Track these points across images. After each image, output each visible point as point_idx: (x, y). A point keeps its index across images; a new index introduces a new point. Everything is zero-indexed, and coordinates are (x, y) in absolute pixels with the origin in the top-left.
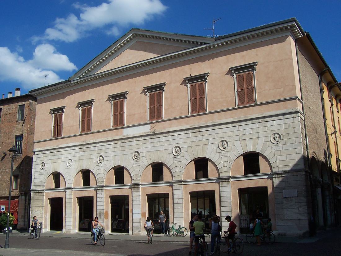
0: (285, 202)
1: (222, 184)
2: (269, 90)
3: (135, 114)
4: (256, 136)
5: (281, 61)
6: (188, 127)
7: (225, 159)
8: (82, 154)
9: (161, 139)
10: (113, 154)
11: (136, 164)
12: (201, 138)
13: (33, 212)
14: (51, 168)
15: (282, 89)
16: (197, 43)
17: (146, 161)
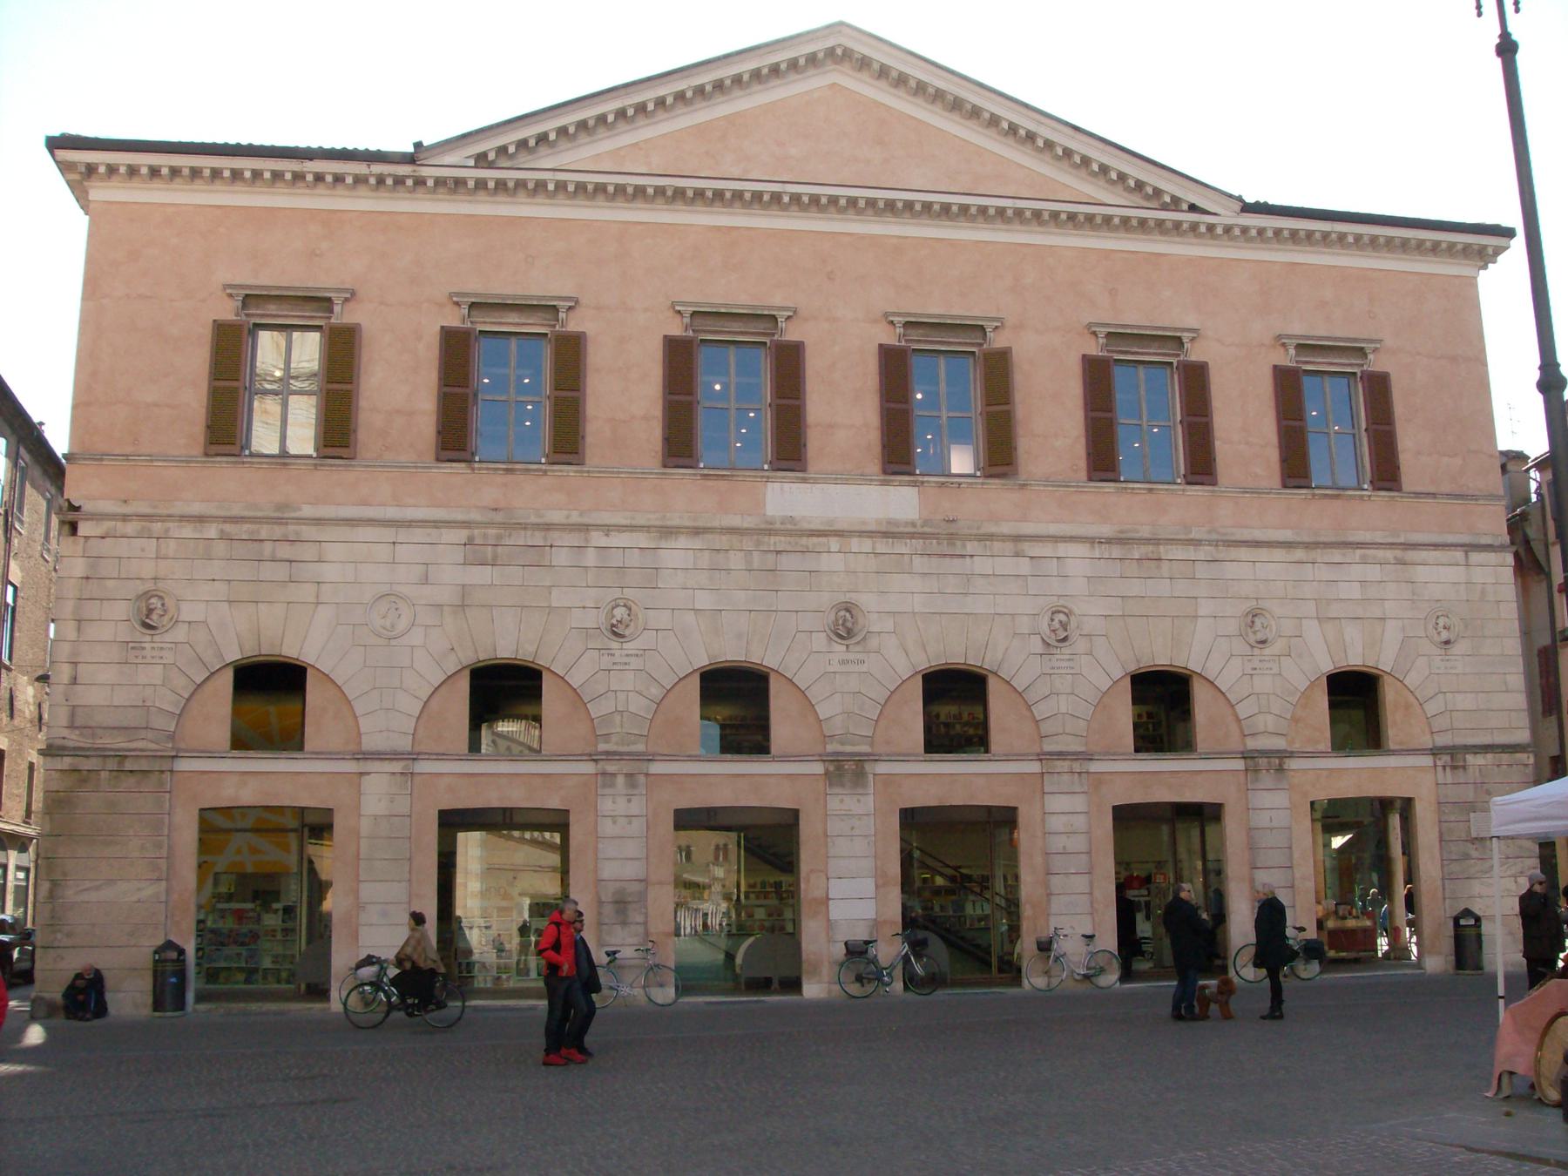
0: (1475, 854)
1: (1257, 780)
3: (831, 426)
4: (1376, 611)
6: (1106, 530)
7: (1263, 684)
8: (480, 575)
9: (981, 565)
10: (704, 600)
11: (844, 662)
12: (1163, 588)
13: (70, 893)
16: (1158, 192)
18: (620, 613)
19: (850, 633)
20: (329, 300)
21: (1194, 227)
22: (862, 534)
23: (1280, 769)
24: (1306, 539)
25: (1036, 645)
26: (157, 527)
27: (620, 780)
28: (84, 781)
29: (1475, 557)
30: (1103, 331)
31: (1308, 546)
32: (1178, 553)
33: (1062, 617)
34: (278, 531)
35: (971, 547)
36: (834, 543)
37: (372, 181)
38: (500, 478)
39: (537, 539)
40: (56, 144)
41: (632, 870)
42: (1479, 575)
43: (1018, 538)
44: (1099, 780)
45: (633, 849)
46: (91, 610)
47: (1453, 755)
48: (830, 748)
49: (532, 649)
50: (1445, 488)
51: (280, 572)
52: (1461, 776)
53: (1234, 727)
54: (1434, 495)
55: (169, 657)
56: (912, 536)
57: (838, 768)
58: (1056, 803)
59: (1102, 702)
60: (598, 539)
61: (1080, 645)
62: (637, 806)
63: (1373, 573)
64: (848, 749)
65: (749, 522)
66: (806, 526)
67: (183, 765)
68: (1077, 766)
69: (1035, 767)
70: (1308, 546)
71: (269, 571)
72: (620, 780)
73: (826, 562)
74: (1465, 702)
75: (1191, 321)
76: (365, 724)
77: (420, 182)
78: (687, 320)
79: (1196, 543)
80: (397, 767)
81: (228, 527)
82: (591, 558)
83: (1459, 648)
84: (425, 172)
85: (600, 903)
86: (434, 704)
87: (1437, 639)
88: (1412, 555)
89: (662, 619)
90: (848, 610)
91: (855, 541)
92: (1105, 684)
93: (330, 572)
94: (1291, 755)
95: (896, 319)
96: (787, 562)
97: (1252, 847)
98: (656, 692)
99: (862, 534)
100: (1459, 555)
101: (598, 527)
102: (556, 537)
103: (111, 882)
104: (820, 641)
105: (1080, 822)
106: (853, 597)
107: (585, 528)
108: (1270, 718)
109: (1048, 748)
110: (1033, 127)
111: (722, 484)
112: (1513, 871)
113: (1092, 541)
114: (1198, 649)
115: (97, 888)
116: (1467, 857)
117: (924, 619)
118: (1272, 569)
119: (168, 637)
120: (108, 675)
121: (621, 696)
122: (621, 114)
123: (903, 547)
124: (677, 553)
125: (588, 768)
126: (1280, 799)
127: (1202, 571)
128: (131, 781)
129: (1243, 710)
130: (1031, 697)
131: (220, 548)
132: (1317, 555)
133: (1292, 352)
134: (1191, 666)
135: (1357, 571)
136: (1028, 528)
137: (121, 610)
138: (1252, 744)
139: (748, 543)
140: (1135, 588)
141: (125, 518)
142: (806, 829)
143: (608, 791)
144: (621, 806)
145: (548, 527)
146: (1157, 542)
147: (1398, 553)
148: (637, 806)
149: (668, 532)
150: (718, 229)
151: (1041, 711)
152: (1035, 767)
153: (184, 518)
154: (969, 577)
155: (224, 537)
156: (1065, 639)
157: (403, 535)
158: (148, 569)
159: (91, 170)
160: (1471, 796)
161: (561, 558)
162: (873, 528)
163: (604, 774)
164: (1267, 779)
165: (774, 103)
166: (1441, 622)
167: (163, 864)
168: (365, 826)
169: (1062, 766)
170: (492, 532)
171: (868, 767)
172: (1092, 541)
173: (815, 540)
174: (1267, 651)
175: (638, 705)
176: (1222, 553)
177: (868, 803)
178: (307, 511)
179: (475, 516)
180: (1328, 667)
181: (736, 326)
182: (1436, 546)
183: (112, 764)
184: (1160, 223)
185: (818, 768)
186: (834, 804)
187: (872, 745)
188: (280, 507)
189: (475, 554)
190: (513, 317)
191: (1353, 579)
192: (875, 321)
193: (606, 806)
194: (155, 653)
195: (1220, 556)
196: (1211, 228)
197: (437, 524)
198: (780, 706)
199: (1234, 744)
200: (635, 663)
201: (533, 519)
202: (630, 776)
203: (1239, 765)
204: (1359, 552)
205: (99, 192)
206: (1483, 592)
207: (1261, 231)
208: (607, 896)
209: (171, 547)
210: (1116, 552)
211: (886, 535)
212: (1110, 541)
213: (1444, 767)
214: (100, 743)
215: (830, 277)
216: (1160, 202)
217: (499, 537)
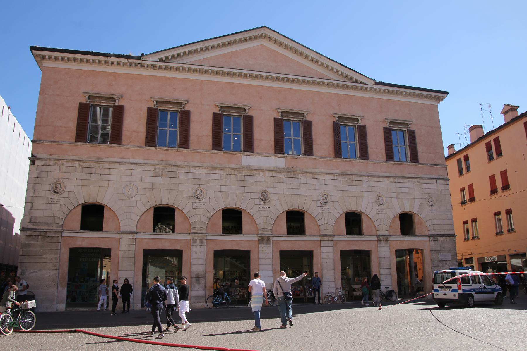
0: (441, 265)
1: (380, 243)
5: (432, 127)
6: (338, 172)
9: (303, 181)
10: (224, 189)
11: (263, 208)
15: (434, 155)
16: (352, 78)
17: (280, 207)
18: (199, 192)
20: (115, 98)
21: (362, 88)
23: (387, 241)
25: (319, 204)
26: (60, 163)
27: (198, 241)
29: (439, 182)
30: (337, 116)
32: (357, 178)
34: (97, 165)
36: (261, 173)
37: (129, 64)
38: (164, 152)
40: (33, 49)
41: (201, 268)
43: (313, 173)
44: (336, 243)
45: (202, 261)
47: (435, 237)
48: (260, 232)
49: (172, 202)
50: (430, 163)
51: (97, 177)
52: (436, 243)
53: (374, 228)
54: (427, 164)
56: (283, 172)
57: (262, 238)
58: (324, 249)
60: (193, 170)
61: (331, 204)
63: (411, 185)
64: (265, 233)
67: (64, 235)
69: (318, 239)
70: (394, 177)
71: (93, 177)
72: (198, 241)
73: (259, 179)
74: (436, 222)
76: (121, 223)
77: (142, 66)
78: (220, 108)
79: (363, 175)
80: (131, 236)
82: (190, 176)
83: (435, 207)
84: (144, 62)
85: (192, 278)
86: (143, 218)
88: (421, 181)
89: (210, 194)
90: (265, 193)
92: (338, 215)
93: (113, 178)
95: (279, 110)
96: (248, 178)
97: (380, 263)
98: (209, 215)
104: (257, 201)
105: (331, 255)
107: (189, 167)
109: (322, 233)
110: (318, 58)
114: (364, 205)
115: (36, 272)
116: (439, 266)
117: (288, 195)
118: (383, 184)
119: (62, 196)
121: (199, 216)
122: (201, 50)
123: (281, 175)
124: (216, 175)
125: (189, 237)
126: (387, 249)
127: (365, 184)
128: (49, 239)
129: (376, 224)
130: (317, 219)
131: (79, 170)
132: (396, 180)
133: (389, 124)
134: (362, 211)
135: (407, 185)
136: (316, 170)
137: (47, 187)
138: (379, 233)
139: (236, 173)
140: (346, 188)
142: (253, 256)
143: (194, 244)
144: (198, 249)
145: (178, 166)
146: (351, 175)
147: (418, 180)
148: (203, 249)
149: (213, 169)
151: (319, 223)
152: (318, 239)
155: (81, 166)
156: (326, 202)
157: (135, 167)
158: (56, 175)
159: (43, 57)
161: (182, 175)
163: (193, 239)
164: (383, 243)
165: (245, 49)
166: (430, 199)
167: (57, 264)
169: (326, 238)
170: (161, 167)
171: (271, 238)
173: (256, 172)
174: (383, 207)
175: (204, 219)
176: (370, 179)
177: (271, 249)
178: (106, 159)
179: (156, 162)
180: (399, 212)
181: (234, 111)
182: (429, 178)
183: (43, 234)
184: (352, 87)
185: (256, 238)
186: (260, 249)
187: (272, 232)
188: (98, 158)
189: (156, 174)
190: (169, 106)
191: (406, 187)
192: (273, 111)
193: (193, 249)
194: (58, 200)
196: (366, 89)
198: (245, 220)
199: (374, 233)
200: (203, 207)
201: (174, 164)
203: (375, 239)
205: (46, 64)
206: (441, 192)
207: (380, 90)
208: (193, 276)
209: (64, 169)
210: (341, 178)
211: (276, 171)
212: (339, 174)
214: (39, 227)
215: (261, 98)
216: (352, 80)
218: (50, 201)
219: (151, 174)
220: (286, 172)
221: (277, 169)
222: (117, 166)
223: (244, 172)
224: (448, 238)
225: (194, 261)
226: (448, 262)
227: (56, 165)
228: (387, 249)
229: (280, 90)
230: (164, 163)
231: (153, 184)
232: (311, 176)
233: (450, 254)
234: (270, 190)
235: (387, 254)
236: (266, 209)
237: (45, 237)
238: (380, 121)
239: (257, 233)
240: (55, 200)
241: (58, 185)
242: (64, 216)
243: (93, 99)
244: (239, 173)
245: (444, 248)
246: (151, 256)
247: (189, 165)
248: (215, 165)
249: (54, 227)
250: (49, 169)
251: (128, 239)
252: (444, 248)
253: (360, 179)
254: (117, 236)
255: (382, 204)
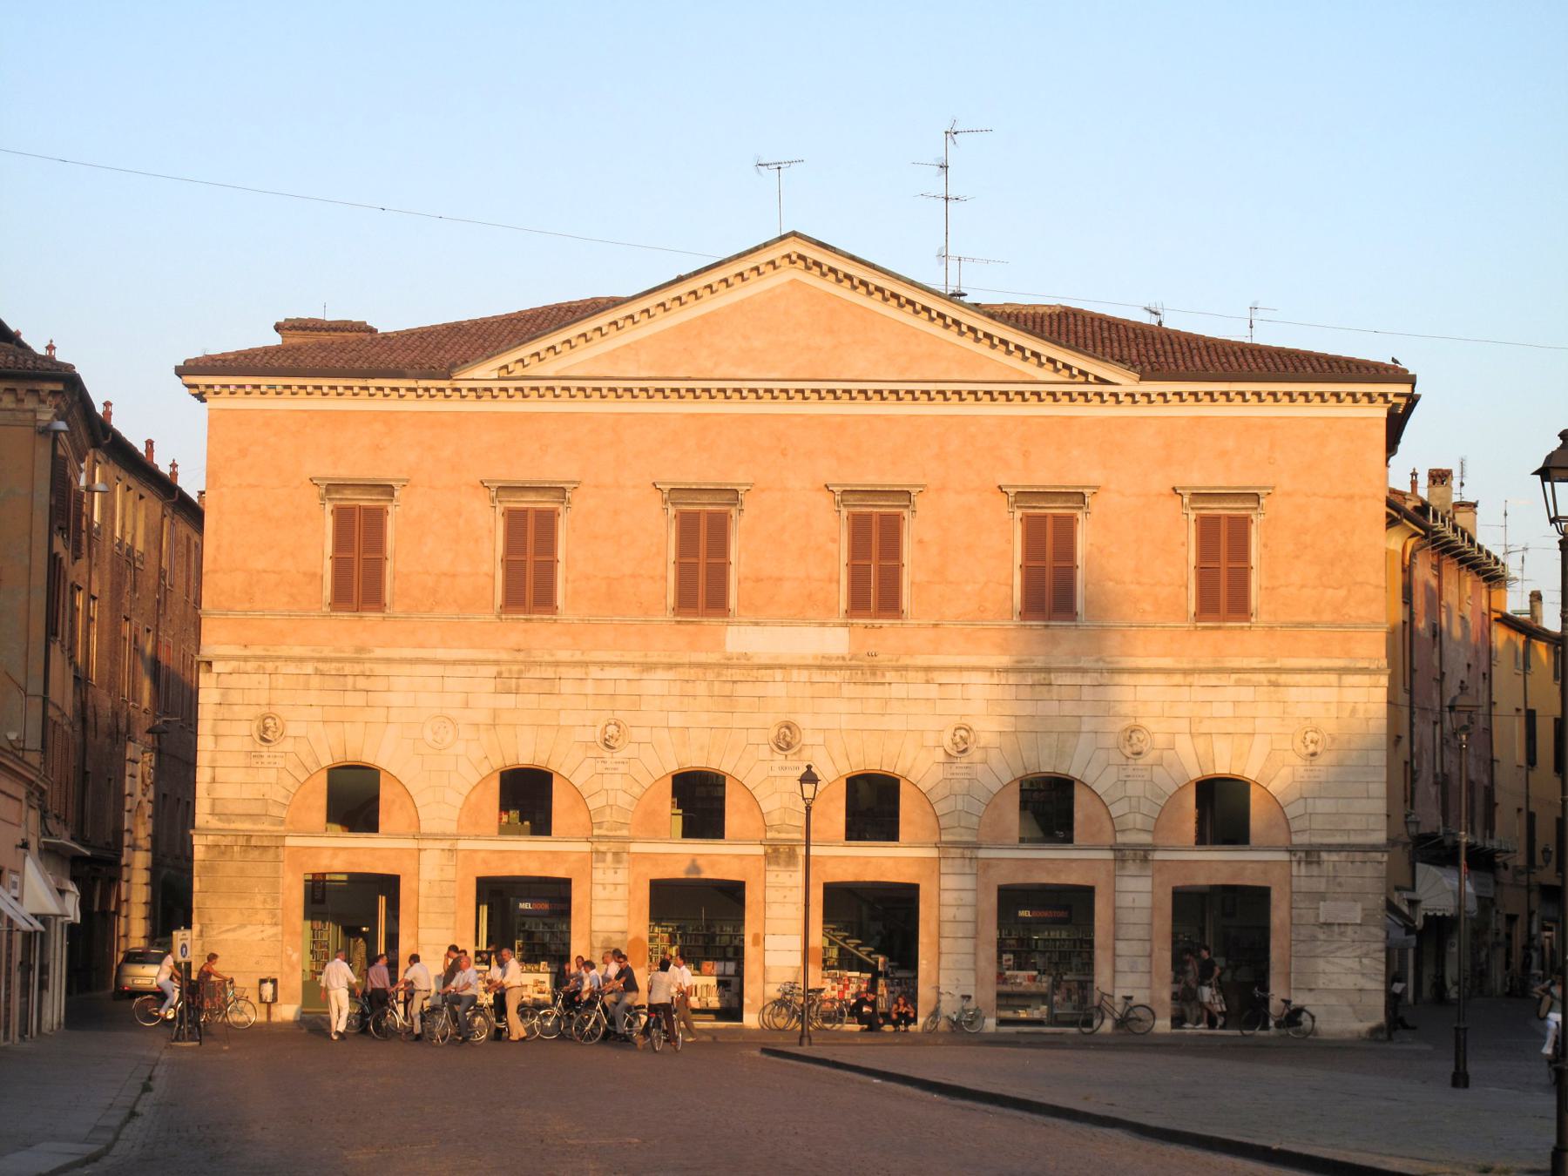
0: (1322, 937)
1: (1123, 868)
2: (1303, 586)
3: (780, 579)
5: (1350, 498)
8: (509, 701)
9: (898, 691)
10: (676, 720)
14: (320, 740)
15: (1343, 593)
18: (612, 730)
19: (789, 746)
22: (799, 667)
23: (1145, 860)
24: (1185, 665)
26: (270, 666)
27: (609, 857)
28: (223, 853)
29: (1349, 679)
30: (1012, 491)
31: (1185, 672)
32: (1067, 679)
33: (963, 733)
34: (357, 668)
35: (890, 676)
36: (779, 675)
38: (522, 626)
39: (549, 673)
41: (618, 924)
42: (1350, 695)
43: (928, 669)
44: (987, 864)
45: (619, 908)
46: (224, 728)
47: (1311, 854)
48: (769, 835)
52: (1315, 870)
53: (1108, 824)
54: (1311, 625)
55: (281, 763)
56: (840, 668)
57: (776, 850)
59: (993, 803)
60: (595, 672)
62: (622, 876)
63: (1246, 693)
64: (783, 836)
65: (713, 658)
66: (756, 661)
68: (968, 853)
70: (1185, 672)
74: (1323, 806)
75: (1094, 476)
79: (1084, 671)
80: (446, 845)
81: (321, 666)
82: (589, 688)
84: (459, 384)
87: (1304, 751)
88: (1283, 678)
91: (795, 672)
93: (396, 699)
94: (1154, 848)
96: (741, 689)
99: (799, 667)
100: (1333, 678)
101: (595, 663)
102: (563, 671)
103: (243, 926)
104: (764, 752)
106: (792, 718)
107: (586, 664)
108: (1139, 817)
109: (944, 838)
111: (691, 628)
112: (1358, 952)
113: (991, 670)
115: (234, 930)
116: (1314, 938)
119: (280, 748)
120: (237, 776)
123: (832, 677)
124: (656, 683)
125: (586, 847)
126: (1145, 884)
127: (1087, 693)
128: (255, 854)
129: (1116, 811)
131: (315, 681)
135: (1231, 693)
137: (244, 728)
138: (1121, 839)
139: (711, 675)
141: (246, 659)
144: (610, 877)
145: (557, 664)
146: (1048, 670)
147: (1273, 677)
149: (648, 667)
150: (693, 415)
153: (288, 659)
154: (887, 701)
156: (965, 751)
157: (449, 671)
158: (263, 697)
160: (1323, 888)
161: (567, 687)
162: (810, 662)
163: (597, 852)
164: (1132, 868)
166: (1309, 737)
168: (423, 888)
170: (515, 668)
172: (991, 670)
175: (623, 800)
178: (379, 653)
179: (504, 656)
181: (705, 498)
182: (1309, 671)
183: (242, 841)
185: (760, 850)
186: (771, 877)
188: (360, 650)
190: (532, 497)
193: (598, 875)
195: (1103, 681)
197: (473, 662)
199: (1107, 838)
200: (622, 768)
201: (547, 658)
202: (616, 854)
203: (1109, 855)
204: (1234, 676)
208: (597, 944)
209: (280, 681)
211: (820, 667)
213: (1299, 862)
214: (233, 826)
215: (784, 454)
217: (520, 672)
218: (254, 761)
219: (490, 685)
220: (849, 668)
221: (826, 662)
222: (406, 669)
223: (729, 674)
224: (1359, 856)
225: (599, 908)
226: (1350, 930)
227: (260, 671)
228: (1145, 884)
229: (840, 425)
230: (520, 657)
231: (495, 712)
232: (921, 676)
233: (1359, 906)
234: (803, 720)
235: (1145, 901)
236: (788, 773)
237: (248, 847)
238: (1161, 494)
239: (762, 836)
240: (265, 760)
241: (270, 723)
242: (287, 797)
243: (337, 492)
244: (719, 675)
245: (1340, 885)
246: (496, 894)
247: (586, 658)
248: (654, 657)
249: (266, 826)
250: (244, 681)
251: (438, 853)
252: (1340, 885)
253: (1077, 679)
254: (412, 844)
255: (1139, 754)
